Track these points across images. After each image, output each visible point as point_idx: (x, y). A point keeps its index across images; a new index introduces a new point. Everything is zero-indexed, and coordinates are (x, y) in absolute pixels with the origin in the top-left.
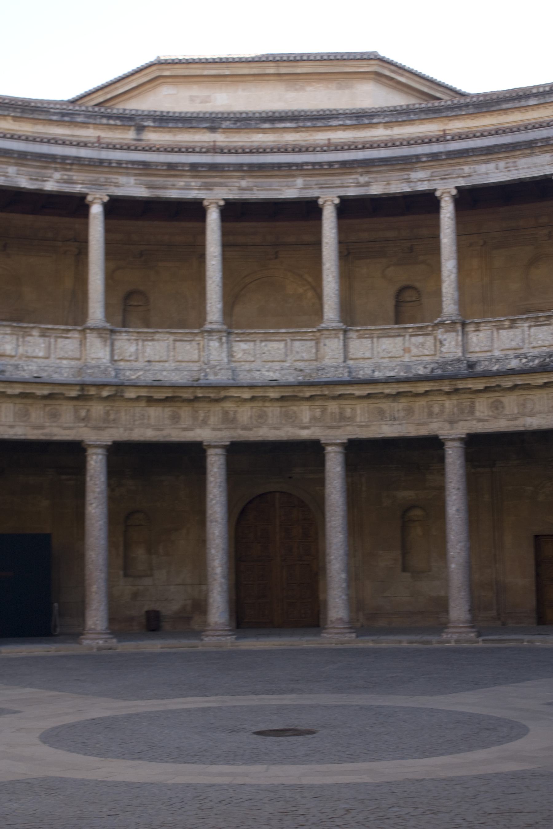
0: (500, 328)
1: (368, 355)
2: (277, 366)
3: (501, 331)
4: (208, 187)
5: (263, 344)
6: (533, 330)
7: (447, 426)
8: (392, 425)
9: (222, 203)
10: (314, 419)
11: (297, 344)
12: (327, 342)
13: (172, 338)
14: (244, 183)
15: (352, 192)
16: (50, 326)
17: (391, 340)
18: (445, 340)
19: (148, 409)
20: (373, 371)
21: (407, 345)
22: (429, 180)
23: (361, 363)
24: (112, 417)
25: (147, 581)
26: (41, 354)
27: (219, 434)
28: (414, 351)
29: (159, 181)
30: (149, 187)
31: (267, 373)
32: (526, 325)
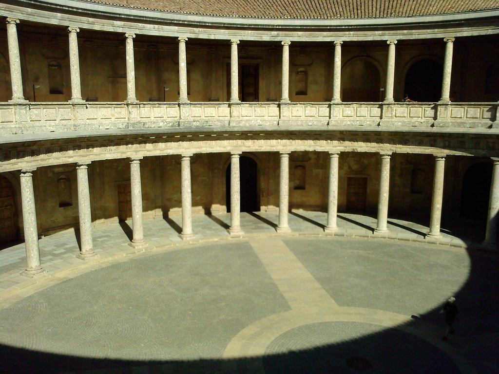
0: (154, 106)
2: (52, 123)
3: (154, 108)
5: (45, 110)
6: (168, 109)
7: (134, 153)
8: (111, 153)
9: (18, 22)
15: (85, 26)
18: (132, 112)
20: (99, 126)
21: (113, 112)
22: (122, 27)
27: (30, 164)
28: (117, 116)
31: (49, 128)
32: (165, 106)
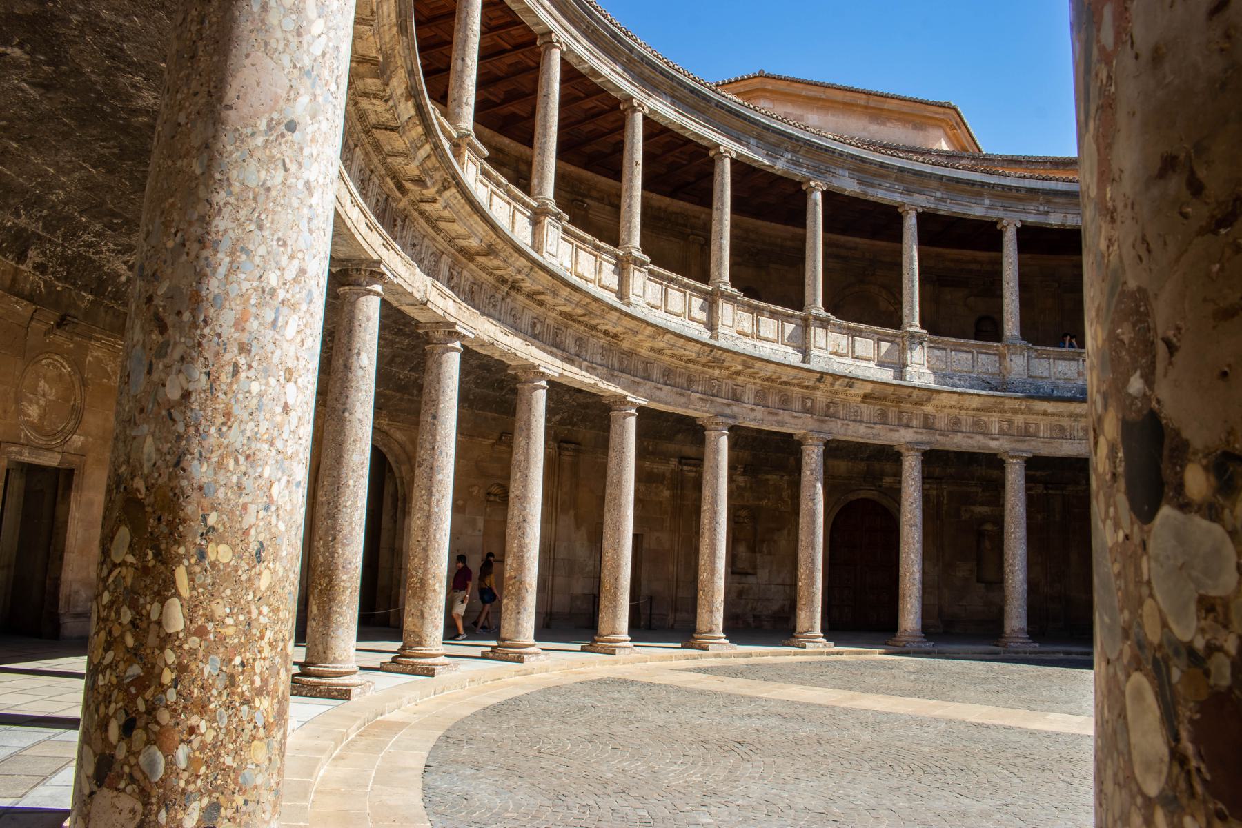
1: (1046, 374)
4: (908, 192)
9: (920, 210)
10: (1001, 429)
11: (982, 357)
12: (1013, 357)
13: (876, 336)
14: (939, 195)
15: (1032, 219)
16: (779, 309)
17: (1066, 363)
19: (862, 405)
23: (1040, 382)
24: (832, 410)
25: (751, 579)
26: (771, 337)
29: (868, 178)
30: (861, 182)
